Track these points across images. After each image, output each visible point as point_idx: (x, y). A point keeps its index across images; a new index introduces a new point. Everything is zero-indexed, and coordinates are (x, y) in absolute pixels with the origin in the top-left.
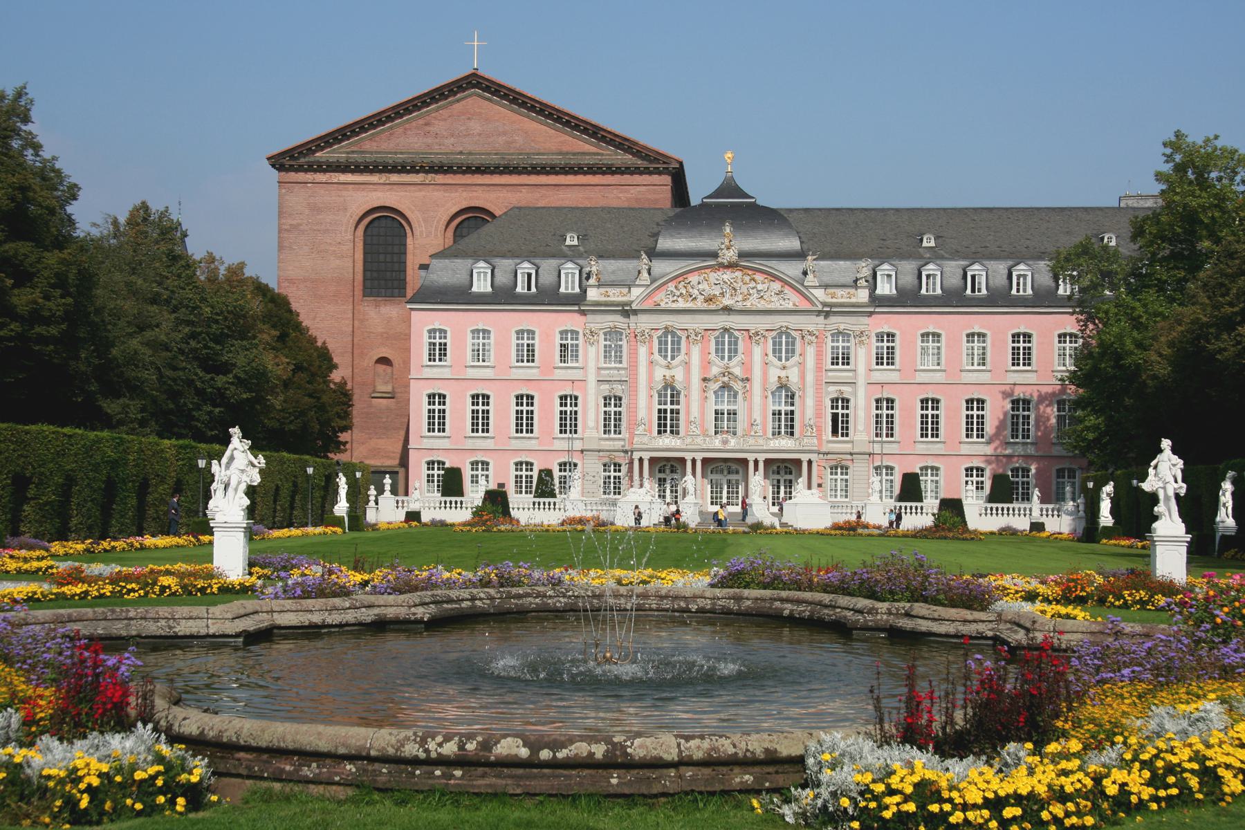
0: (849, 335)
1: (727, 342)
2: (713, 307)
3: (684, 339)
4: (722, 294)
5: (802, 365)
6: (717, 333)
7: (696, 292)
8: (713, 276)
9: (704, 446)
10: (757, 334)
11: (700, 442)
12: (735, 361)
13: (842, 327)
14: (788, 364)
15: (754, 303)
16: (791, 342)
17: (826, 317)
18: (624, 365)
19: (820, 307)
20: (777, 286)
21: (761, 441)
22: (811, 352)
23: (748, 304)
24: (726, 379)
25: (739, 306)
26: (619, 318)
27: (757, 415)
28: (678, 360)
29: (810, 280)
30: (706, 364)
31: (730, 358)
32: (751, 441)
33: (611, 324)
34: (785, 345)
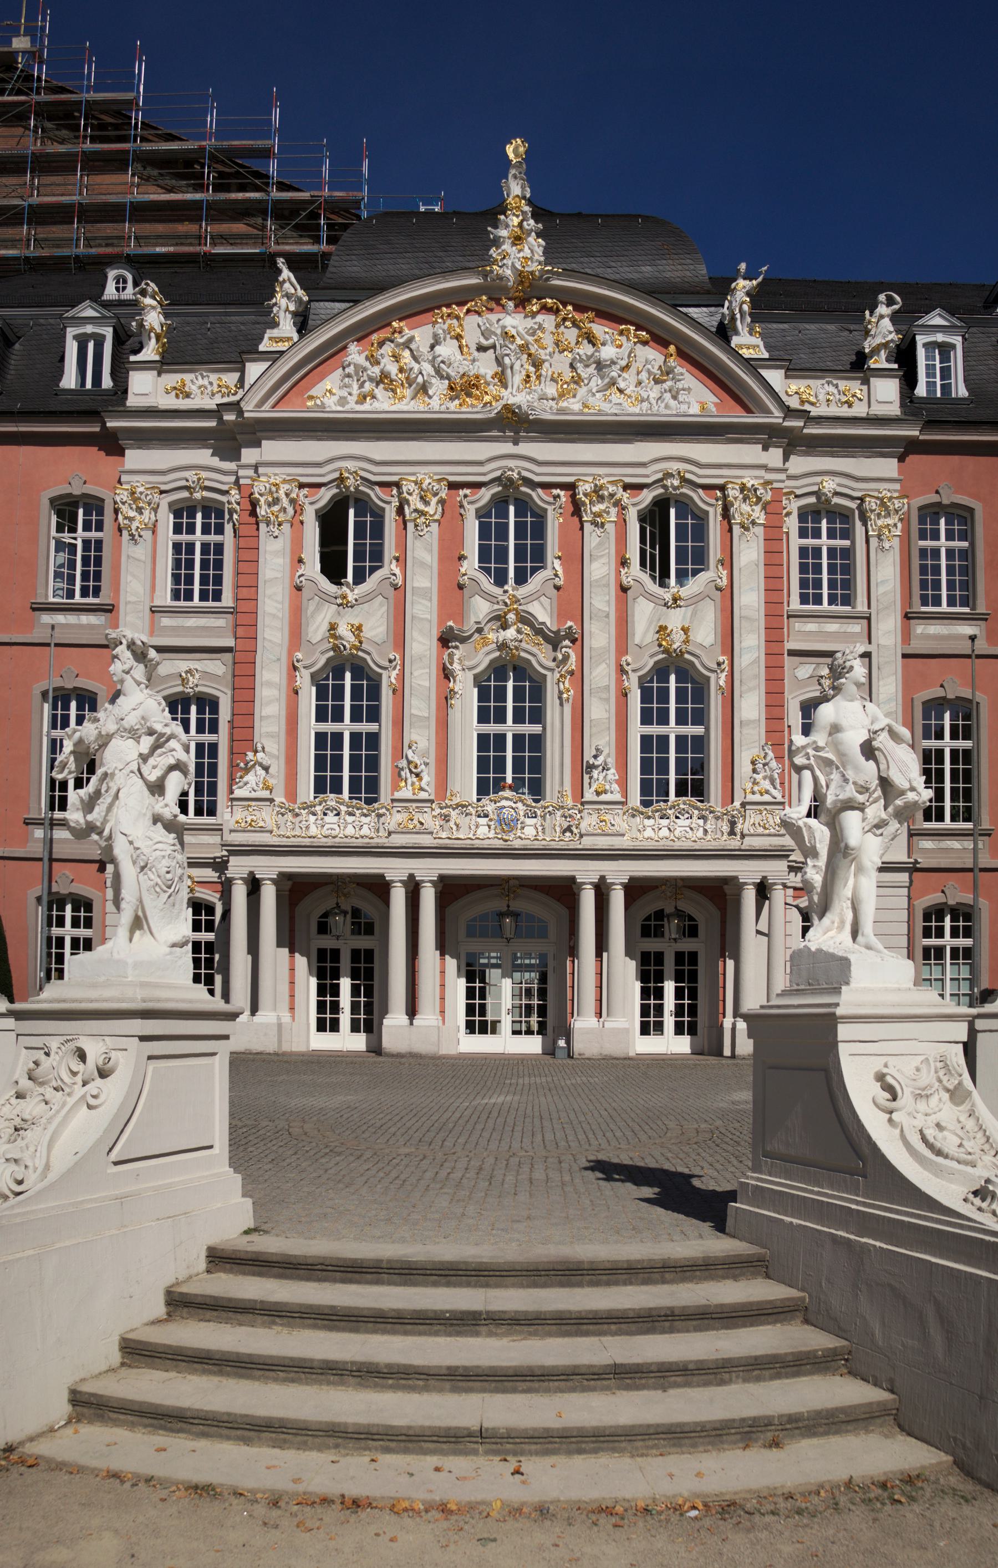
1: (515, 530)
5: (728, 594)
8: (472, 327)
9: (443, 837)
11: (433, 828)
12: (535, 582)
14: (685, 592)
16: (697, 528)
21: (620, 821)
23: (574, 405)
26: (203, 456)
27: (601, 739)
28: (372, 581)
29: (748, 342)
30: (454, 591)
31: (521, 579)
32: (589, 822)
34: (671, 535)
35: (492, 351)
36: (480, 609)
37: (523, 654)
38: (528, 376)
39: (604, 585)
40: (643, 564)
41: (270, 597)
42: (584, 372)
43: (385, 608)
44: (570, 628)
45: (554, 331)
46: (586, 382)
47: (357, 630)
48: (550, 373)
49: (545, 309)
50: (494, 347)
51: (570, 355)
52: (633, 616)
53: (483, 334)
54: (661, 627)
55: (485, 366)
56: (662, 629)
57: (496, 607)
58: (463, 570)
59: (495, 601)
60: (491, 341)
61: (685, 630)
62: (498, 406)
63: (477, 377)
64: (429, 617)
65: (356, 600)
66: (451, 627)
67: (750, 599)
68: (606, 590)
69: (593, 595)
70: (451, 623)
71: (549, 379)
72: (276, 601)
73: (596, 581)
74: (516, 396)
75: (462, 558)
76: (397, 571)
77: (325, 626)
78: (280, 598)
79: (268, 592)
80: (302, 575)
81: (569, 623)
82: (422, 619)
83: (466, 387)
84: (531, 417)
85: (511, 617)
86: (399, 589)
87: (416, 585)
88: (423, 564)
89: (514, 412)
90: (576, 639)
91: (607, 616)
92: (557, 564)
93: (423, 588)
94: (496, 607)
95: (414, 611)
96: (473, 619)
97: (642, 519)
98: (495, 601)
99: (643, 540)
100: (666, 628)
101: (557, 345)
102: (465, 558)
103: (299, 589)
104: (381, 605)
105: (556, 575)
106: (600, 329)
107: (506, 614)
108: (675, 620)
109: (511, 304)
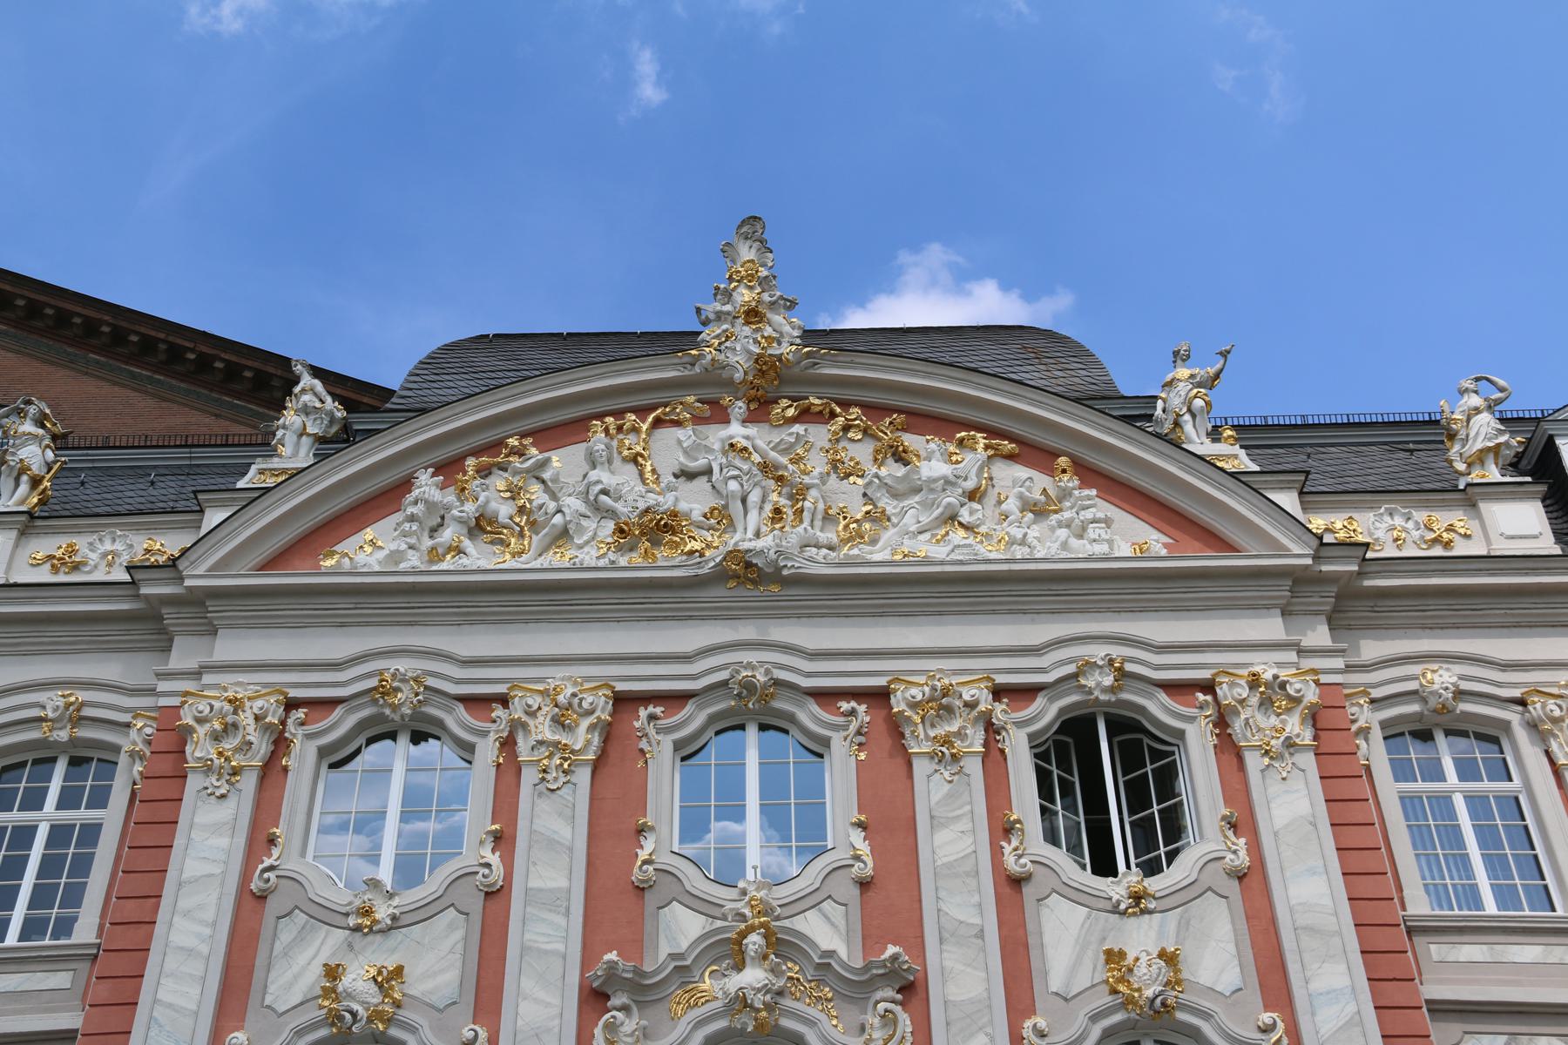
0: (1491, 736)
2: (667, 562)
3: (487, 751)
4: (721, 518)
5: (1252, 880)
6: (694, 718)
7: (573, 504)
8: (670, 447)
10: (940, 704)
13: (1443, 678)
14: (1155, 884)
15: (909, 541)
17: (1335, 623)
18: (85, 931)
19: (1298, 553)
20: (1016, 479)
22: (1291, 802)
24: (753, 976)
25: (818, 564)
30: (617, 896)
33: (53, 701)
35: (705, 478)
36: (682, 928)
37: (786, 1023)
38: (777, 511)
39: (967, 874)
40: (1051, 837)
41: (187, 914)
42: (889, 505)
43: (459, 934)
44: (895, 958)
45: (828, 446)
46: (895, 520)
47: (388, 980)
48: (821, 506)
49: (805, 415)
50: (708, 472)
51: (860, 481)
52: (1041, 934)
53: (685, 452)
54: (1109, 953)
55: (694, 501)
56: (1114, 957)
57: (719, 924)
58: (643, 855)
59: (717, 912)
60: (701, 463)
61: (1169, 958)
62: (714, 557)
63: (674, 514)
64: (560, 947)
65: (394, 918)
66: (612, 965)
67: (1310, 889)
68: (973, 883)
69: (942, 894)
70: (612, 956)
71: (819, 516)
72: (202, 922)
73: (949, 865)
74: (753, 535)
75: (640, 831)
76: (494, 859)
77: (313, 976)
78: (209, 915)
79: (183, 904)
80: (271, 868)
81: (891, 950)
82: (546, 952)
83: (662, 528)
84: (785, 572)
85: (754, 941)
86: (496, 895)
87: (533, 883)
88: (552, 844)
89: (749, 565)
90: (911, 989)
91: (981, 934)
92: (857, 838)
93: (551, 891)
94: (719, 924)
95: (527, 936)
96: (664, 950)
97: (1041, 756)
98: (717, 912)
99: (1045, 791)
100: (1122, 955)
101: (835, 468)
102: (652, 829)
103: (262, 898)
104: (451, 927)
105: (857, 858)
106: (911, 440)
107: (743, 935)
108: (1142, 940)
109: (739, 408)
